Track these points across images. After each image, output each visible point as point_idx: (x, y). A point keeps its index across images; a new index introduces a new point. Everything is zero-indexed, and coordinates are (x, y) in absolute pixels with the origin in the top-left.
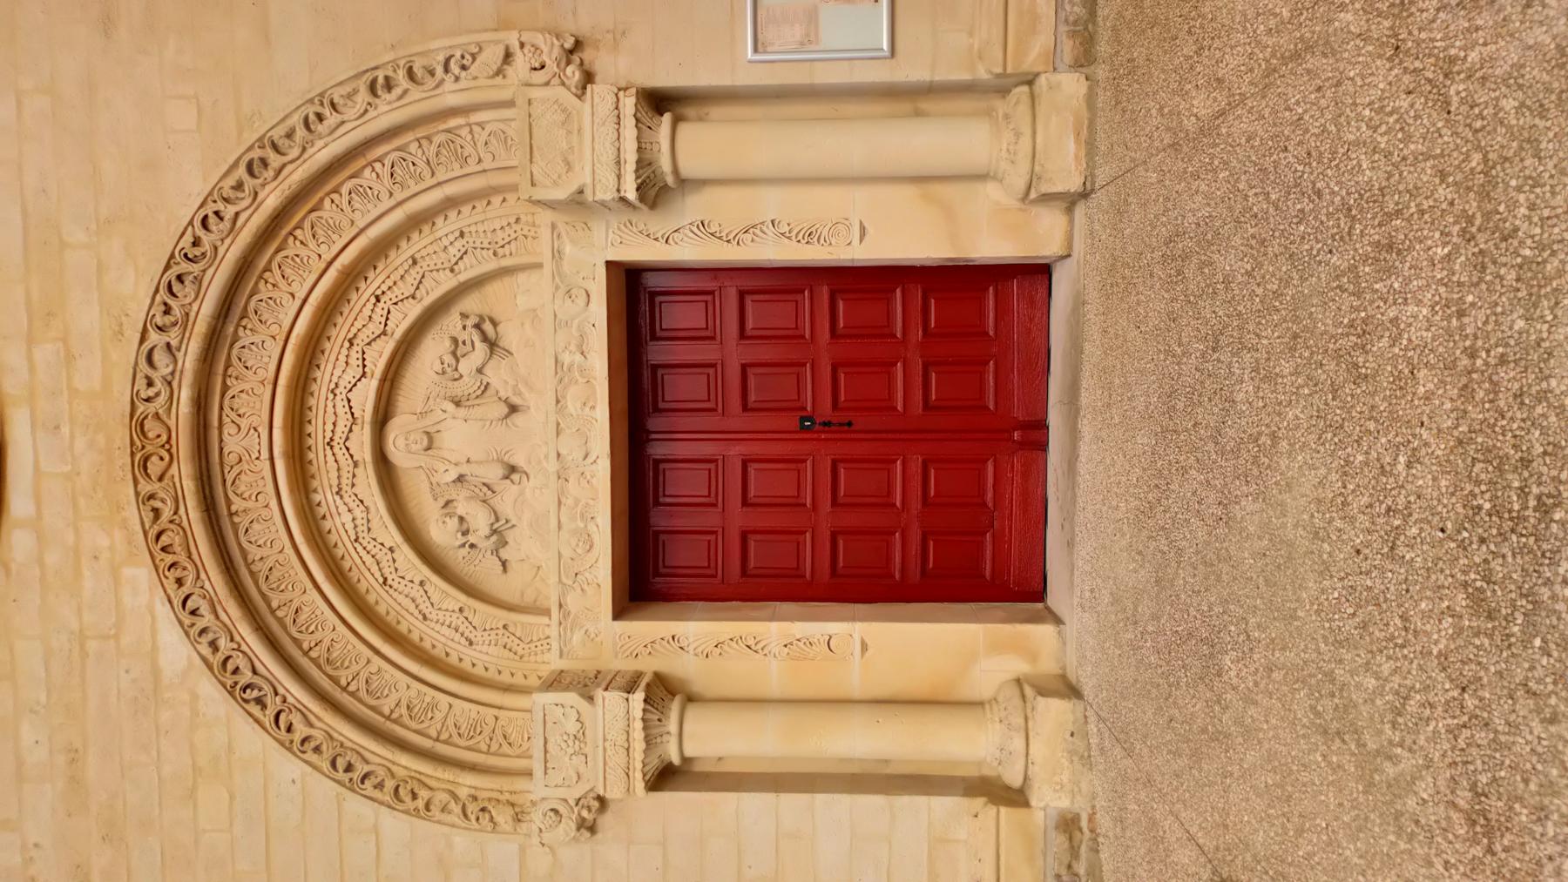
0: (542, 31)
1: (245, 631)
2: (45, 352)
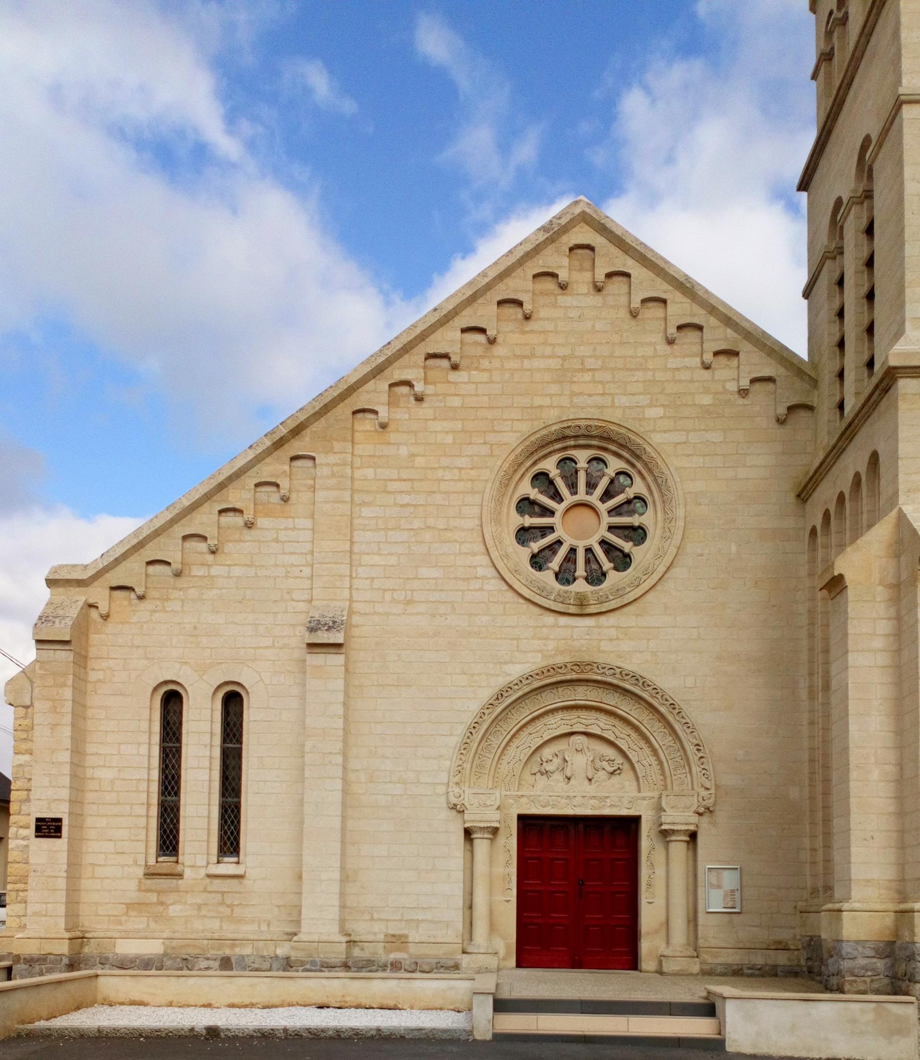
0: (715, 801)
1: (520, 693)
2: (613, 632)
